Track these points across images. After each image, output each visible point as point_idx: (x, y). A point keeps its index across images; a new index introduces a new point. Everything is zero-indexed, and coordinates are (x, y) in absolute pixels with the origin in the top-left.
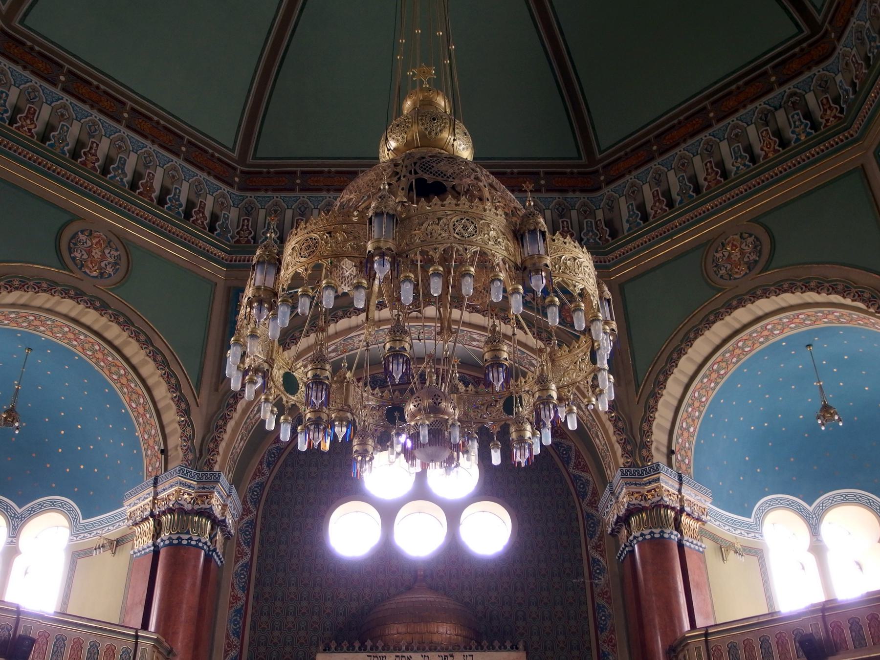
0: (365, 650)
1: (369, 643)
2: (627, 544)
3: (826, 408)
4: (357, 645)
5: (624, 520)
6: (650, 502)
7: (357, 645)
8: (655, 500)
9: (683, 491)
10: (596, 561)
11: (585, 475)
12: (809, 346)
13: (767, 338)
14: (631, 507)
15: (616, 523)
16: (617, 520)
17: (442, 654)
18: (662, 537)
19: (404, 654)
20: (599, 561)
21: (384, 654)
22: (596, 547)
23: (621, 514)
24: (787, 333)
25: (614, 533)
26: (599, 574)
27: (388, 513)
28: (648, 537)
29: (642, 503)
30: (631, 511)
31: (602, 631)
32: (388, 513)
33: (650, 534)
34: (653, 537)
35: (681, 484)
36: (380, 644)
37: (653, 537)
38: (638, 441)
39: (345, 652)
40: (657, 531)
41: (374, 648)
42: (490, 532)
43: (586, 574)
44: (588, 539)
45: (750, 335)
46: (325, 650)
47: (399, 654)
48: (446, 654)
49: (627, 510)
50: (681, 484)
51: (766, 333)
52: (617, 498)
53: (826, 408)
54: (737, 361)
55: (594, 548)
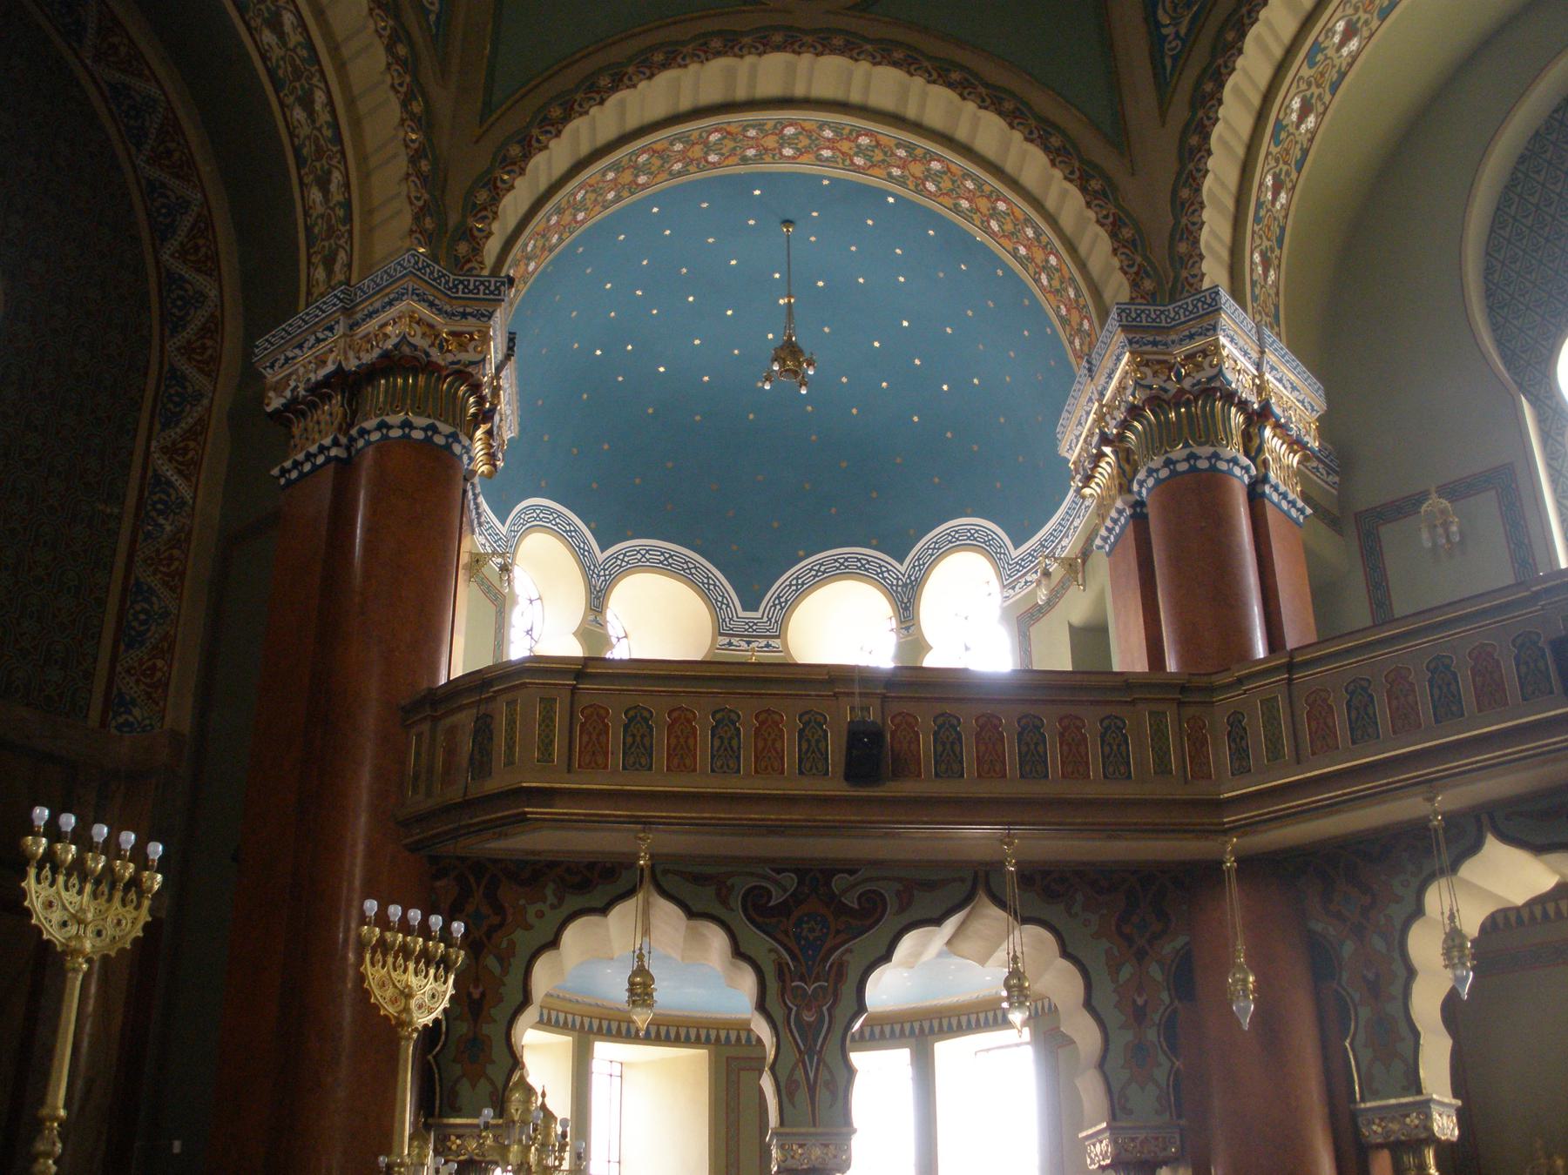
2: (343, 440)
3: (790, 351)
5: (349, 385)
6: (450, 358)
9: (503, 374)
10: (161, 482)
11: (201, 281)
12: (788, 222)
13: (759, 158)
14: (406, 350)
15: (315, 389)
16: (328, 377)
18: (448, 447)
20: (169, 483)
22: (170, 451)
23: (352, 364)
24: (806, 167)
25: (295, 409)
26: (160, 513)
28: (418, 435)
30: (394, 363)
31: (129, 646)
33: (425, 429)
34: (428, 440)
35: (508, 357)
37: (428, 440)
38: (453, 219)
40: (445, 428)
44: (158, 427)
45: (745, 129)
49: (386, 355)
50: (508, 357)
51: (771, 142)
52: (351, 327)
53: (790, 351)
54: (680, 174)
55: (164, 450)
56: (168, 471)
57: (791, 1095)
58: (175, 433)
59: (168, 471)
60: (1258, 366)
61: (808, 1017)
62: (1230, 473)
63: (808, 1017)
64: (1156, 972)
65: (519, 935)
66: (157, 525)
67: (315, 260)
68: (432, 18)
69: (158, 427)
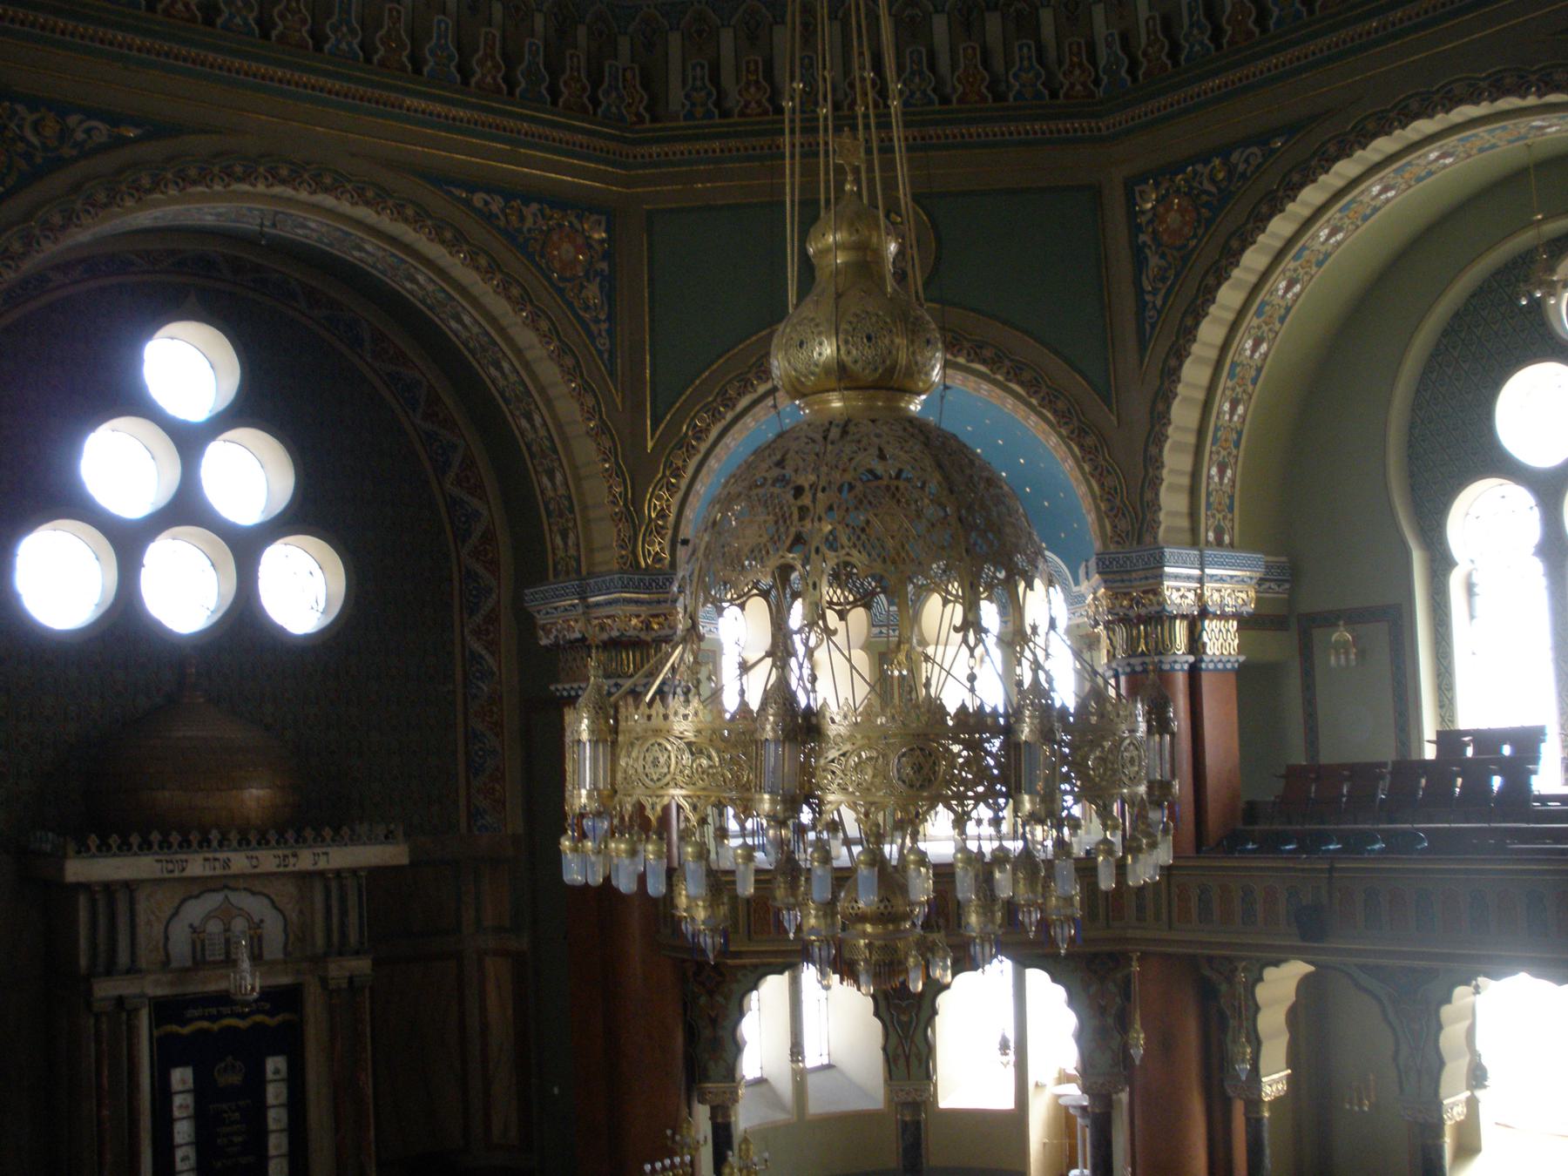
0: (150, 847)
1: (155, 837)
4: (135, 839)
6: (654, 634)
7: (135, 839)
8: (663, 633)
17: (280, 853)
19: (218, 855)
20: (481, 657)
21: (184, 857)
27: (127, 542)
29: (643, 635)
32: (127, 542)
36: (175, 838)
39: (114, 855)
41: (165, 844)
42: (302, 590)
43: (459, 676)
44: (466, 616)
46: (79, 852)
47: (210, 855)
48: (288, 852)
56: (478, 647)
57: (895, 1061)
58: (478, 618)
59: (478, 647)
60: (1201, 580)
61: (904, 1018)
62: (1172, 669)
63: (904, 1018)
64: (1112, 988)
65: (735, 986)
66: (479, 688)
67: (555, 528)
68: (606, 356)
69: (466, 616)
